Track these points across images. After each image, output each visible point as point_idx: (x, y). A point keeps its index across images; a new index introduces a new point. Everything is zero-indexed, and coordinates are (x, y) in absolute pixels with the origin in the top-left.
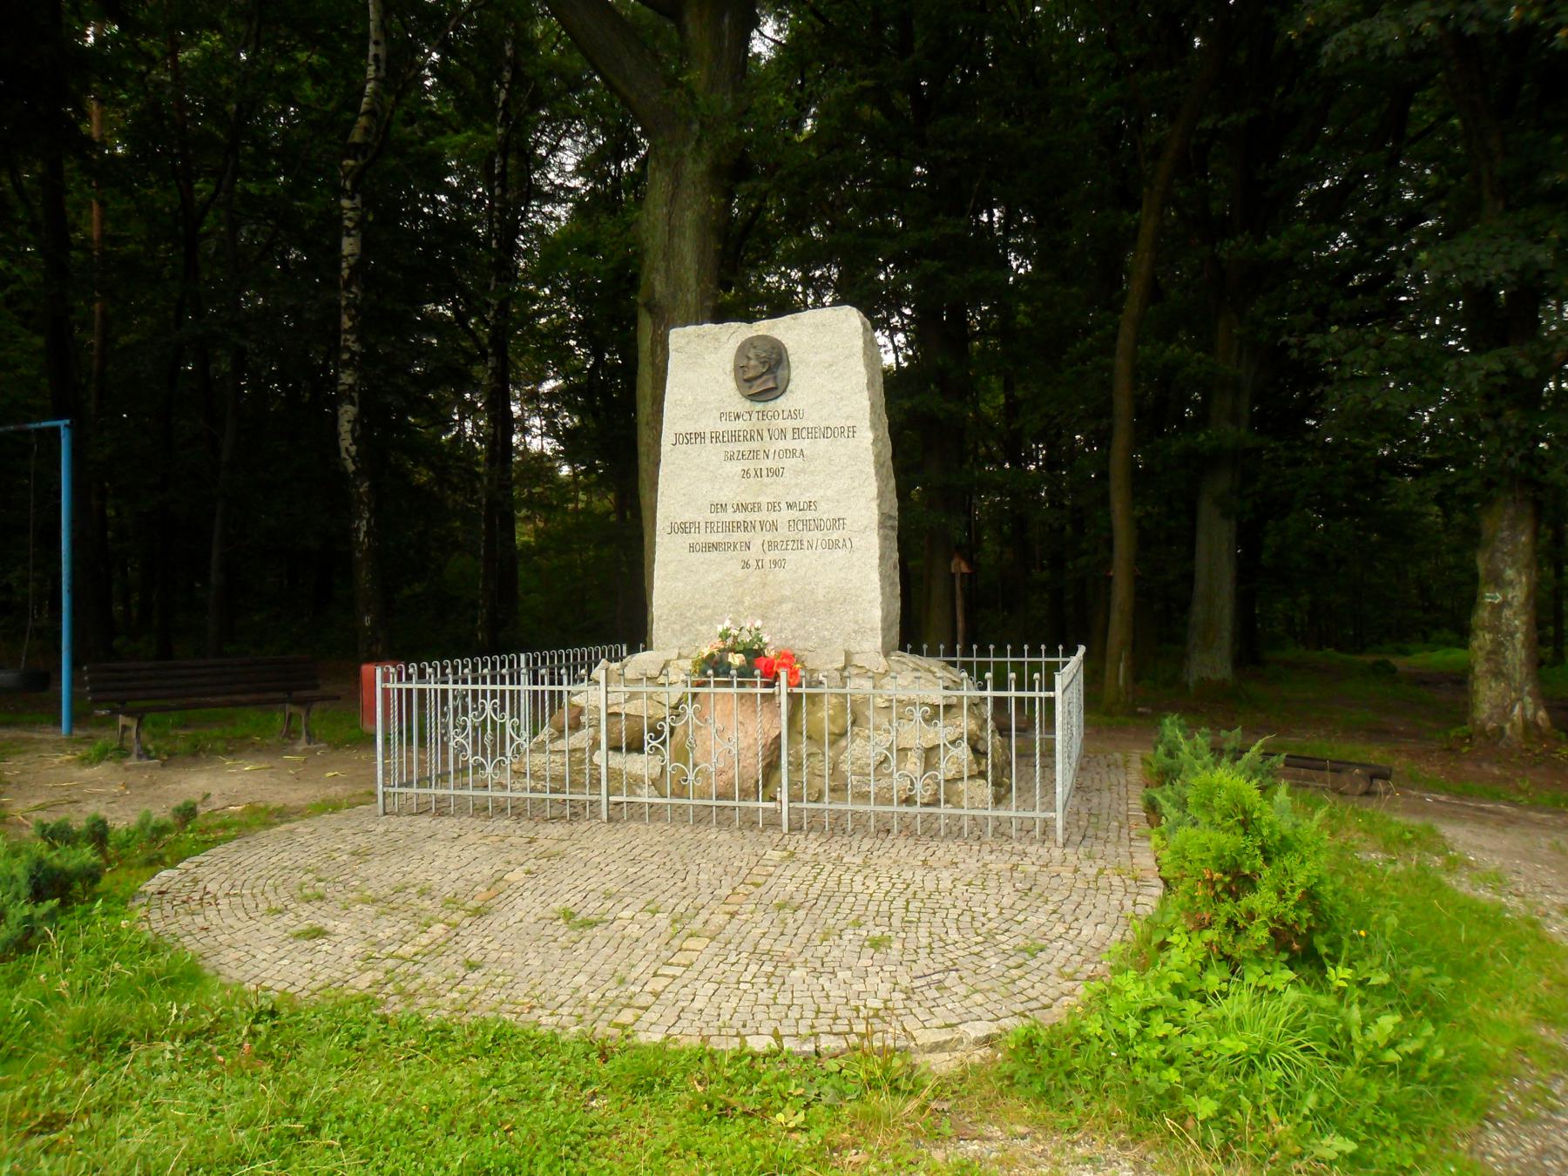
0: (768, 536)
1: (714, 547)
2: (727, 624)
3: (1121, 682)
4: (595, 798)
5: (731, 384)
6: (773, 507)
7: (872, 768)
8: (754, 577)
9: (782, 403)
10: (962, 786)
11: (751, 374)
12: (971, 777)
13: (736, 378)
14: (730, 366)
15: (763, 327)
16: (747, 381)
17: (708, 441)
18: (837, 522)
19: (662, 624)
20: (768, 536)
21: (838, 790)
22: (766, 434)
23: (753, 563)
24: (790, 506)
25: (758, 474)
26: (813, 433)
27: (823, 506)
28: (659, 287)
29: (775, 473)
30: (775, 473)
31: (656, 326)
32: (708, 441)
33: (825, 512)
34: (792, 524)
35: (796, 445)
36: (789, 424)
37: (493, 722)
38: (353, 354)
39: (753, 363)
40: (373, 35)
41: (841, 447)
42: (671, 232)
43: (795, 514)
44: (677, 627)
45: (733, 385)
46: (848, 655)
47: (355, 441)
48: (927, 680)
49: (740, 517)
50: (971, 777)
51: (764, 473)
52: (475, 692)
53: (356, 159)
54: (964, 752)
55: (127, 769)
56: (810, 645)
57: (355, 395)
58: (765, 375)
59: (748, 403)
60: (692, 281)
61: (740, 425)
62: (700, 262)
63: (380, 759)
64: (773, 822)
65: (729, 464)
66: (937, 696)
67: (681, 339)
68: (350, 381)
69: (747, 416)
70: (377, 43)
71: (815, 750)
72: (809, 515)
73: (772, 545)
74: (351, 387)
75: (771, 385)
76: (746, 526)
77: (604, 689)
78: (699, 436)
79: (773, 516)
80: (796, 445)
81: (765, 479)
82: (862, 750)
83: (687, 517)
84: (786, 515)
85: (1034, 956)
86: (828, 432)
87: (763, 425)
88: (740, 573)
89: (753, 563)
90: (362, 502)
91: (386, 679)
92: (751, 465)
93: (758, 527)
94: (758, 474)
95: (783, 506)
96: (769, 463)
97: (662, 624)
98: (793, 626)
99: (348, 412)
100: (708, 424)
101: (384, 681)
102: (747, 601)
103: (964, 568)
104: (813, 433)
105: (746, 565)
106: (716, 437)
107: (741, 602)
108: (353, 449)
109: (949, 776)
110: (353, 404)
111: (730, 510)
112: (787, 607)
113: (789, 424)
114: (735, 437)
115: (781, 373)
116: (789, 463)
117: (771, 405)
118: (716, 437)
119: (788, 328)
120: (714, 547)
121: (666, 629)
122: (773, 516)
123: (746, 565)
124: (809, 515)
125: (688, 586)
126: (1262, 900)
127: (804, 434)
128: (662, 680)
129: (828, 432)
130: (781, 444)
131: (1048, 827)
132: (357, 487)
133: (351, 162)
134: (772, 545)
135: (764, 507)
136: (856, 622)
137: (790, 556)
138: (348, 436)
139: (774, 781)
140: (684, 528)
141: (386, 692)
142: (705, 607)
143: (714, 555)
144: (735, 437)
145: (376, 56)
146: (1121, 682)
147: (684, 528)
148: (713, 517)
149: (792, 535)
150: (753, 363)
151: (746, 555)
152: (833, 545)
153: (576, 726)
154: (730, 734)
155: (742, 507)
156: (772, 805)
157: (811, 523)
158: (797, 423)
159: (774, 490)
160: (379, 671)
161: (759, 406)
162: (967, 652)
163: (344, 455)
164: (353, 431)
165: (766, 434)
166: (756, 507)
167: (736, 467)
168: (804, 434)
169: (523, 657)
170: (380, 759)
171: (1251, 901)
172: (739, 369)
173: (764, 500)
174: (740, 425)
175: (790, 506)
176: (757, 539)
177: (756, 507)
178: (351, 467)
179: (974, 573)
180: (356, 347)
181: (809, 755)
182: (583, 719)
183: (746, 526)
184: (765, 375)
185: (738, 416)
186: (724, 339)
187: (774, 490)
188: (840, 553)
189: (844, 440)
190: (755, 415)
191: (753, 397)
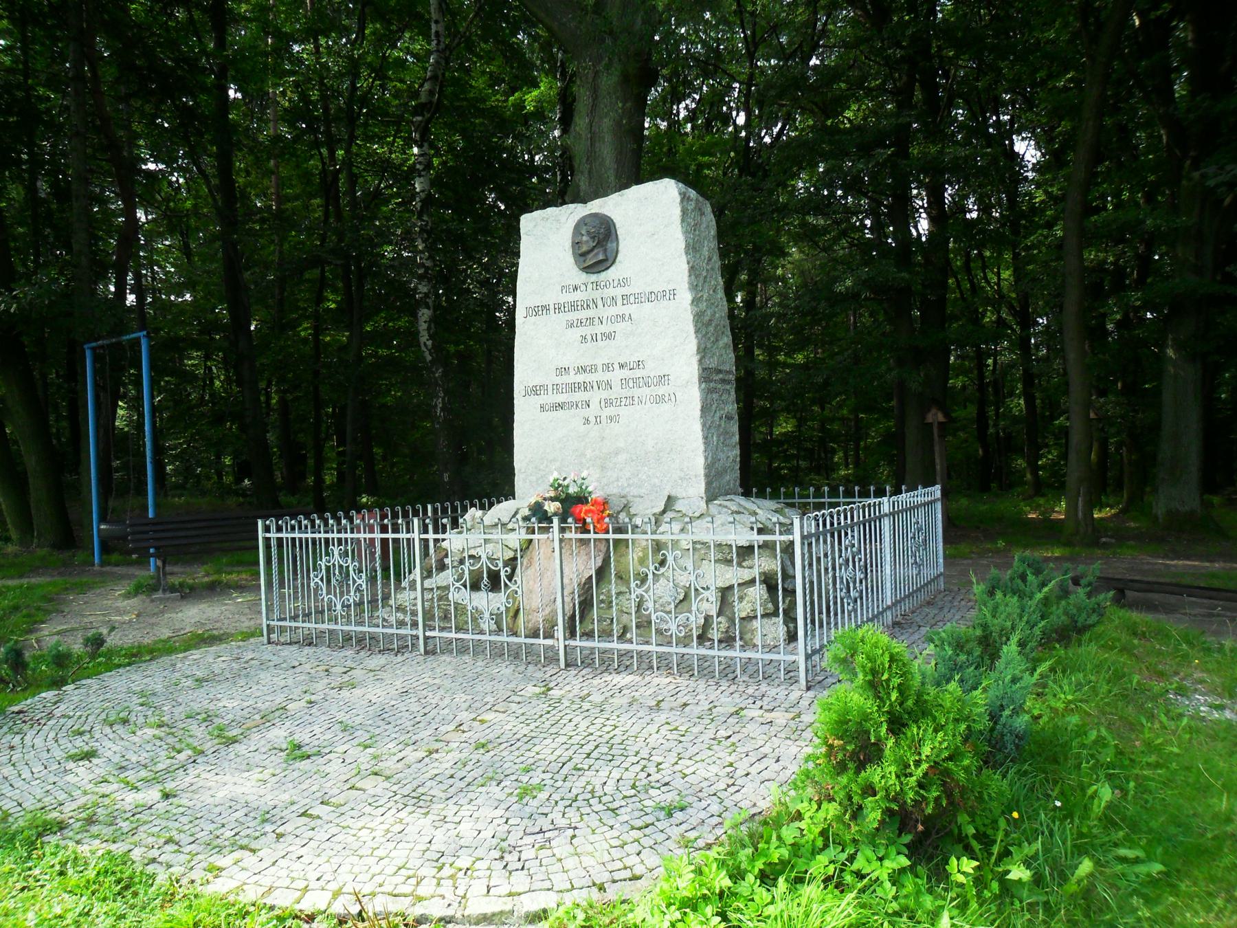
1: (560, 406)
2: (556, 475)
3: (1080, 514)
4: (414, 632)
5: (569, 259)
6: (608, 367)
7: (672, 606)
8: (594, 430)
9: (612, 273)
10: (756, 624)
11: (585, 248)
12: (763, 616)
14: (568, 244)
15: (595, 206)
16: (583, 255)
17: (552, 311)
18: (663, 379)
19: (522, 476)
20: (604, 394)
21: (644, 624)
22: (600, 303)
23: (592, 419)
24: (622, 366)
25: (594, 338)
26: (638, 298)
27: (649, 365)
29: (609, 336)
30: (609, 336)
32: (552, 311)
33: (652, 369)
34: (624, 382)
35: (626, 310)
36: (619, 292)
37: (341, 566)
38: (427, 268)
39: (585, 238)
40: (434, 16)
41: (662, 309)
42: (592, 140)
43: (626, 373)
45: (572, 260)
46: (670, 500)
47: (431, 337)
48: (738, 522)
49: (580, 378)
50: (763, 616)
51: (599, 337)
52: (327, 540)
53: (423, 115)
54: (758, 593)
55: (152, 601)
56: (643, 491)
57: (430, 301)
58: (597, 247)
59: (584, 277)
60: (612, 178)
62: (618, 162)
63: (263, 597)
64: (552, 659)
66: (746, 537)
67: (529, 223)
68: (425, 290)
69: (583, 287)
70: (437, 22)
71: (624, 589)
72: (638, 373)
73: (609, 402)
74: (427, 295)
75: (601, 257)
76: (585, 387)
77: (480, 534)
78: (545, 308)
79: (607, 376)
80: (626, 310)
82: (661, 592)
83: (537, 381)
84: (619, 374)
85: (670, 815)
86: (652, 297)
87: (597, 295)
88: (583, 428)
89: (592, 419)
90: (437, 384)
91: (267, 529)
92: (587, 331)
93: (596, 387)
94: (594, 338)
95: (616, 366)
96: (600, 329)
97: (522, 476)
98: (628, 475)
99: (425, 314)
100: (553, 297)
101: (266, 532)
102: (589, 453)
103: (941, 417)
104: (638, 298)
105: (587, 421)
106: (559, 308)
107: (584, 455)
108: (429, 343)
109: (743, 615)
110: (428, 308)
111: (572, 372)
112: (622, 457)
113: (619, 292)
114: (574, 306)
115: (611, 246)
116: (619, 327)
117: (603, 274)
118: (559, 308)
120: (560, 406)
121: (525, 481)
122: (607, 376)
123: (587, 421)
124: (638, 373)
125: (543, 444)
126: (882, 775)
127: (632, 298)
128: (510, 526)
129: (652, 297)
130: (613, 311)
131: (791, 670)
132: (434, 373)
133: (419, 118)
134: (609, 402)
135: (600, 368)
136: (682, 470)
137: (623, 411)
138: (425, 333)
139: (588, 620)
140: (535, 391)
141: (267, 540)
142: (554, 460)
144: (574, 306)
145: (437, 32)
146: (1080, 514)
147: (535, 391)
148: (559, 380)
149: (625, 393)
150: (585, 238)
152: (659, 400)
153: (442, 567)
154: (552, 574)
155: (583, 369)
156: (549, 642)
157: (641, 380)
158: (625, 291)
159: (605, 353)
160: (260, 522)
161: (594, 277)
163: (424, 349)
164: (429, 329)
165: (600, 303)
166: (593, 369)
167: (577, 333)
168: (632, 298)
169: (429, 507)
170: (263, 597)
171: (874, 774)
172: (576, 244)
173: (599, 362)
174: (578, 296)
175: (622, 366)
176: (595, 396)
177: (593, 369)
178: (429, 358)
179: (793, 423)
180: (428, 263)
181: (618, 594)
182: (447, 561)
183: (585, 387)
185: (576, 288)
186: (563, 219)
187: (605, 353)
188: (665, 407)
189: (666, 302)
190: (590, 286)
191: (588, 269)
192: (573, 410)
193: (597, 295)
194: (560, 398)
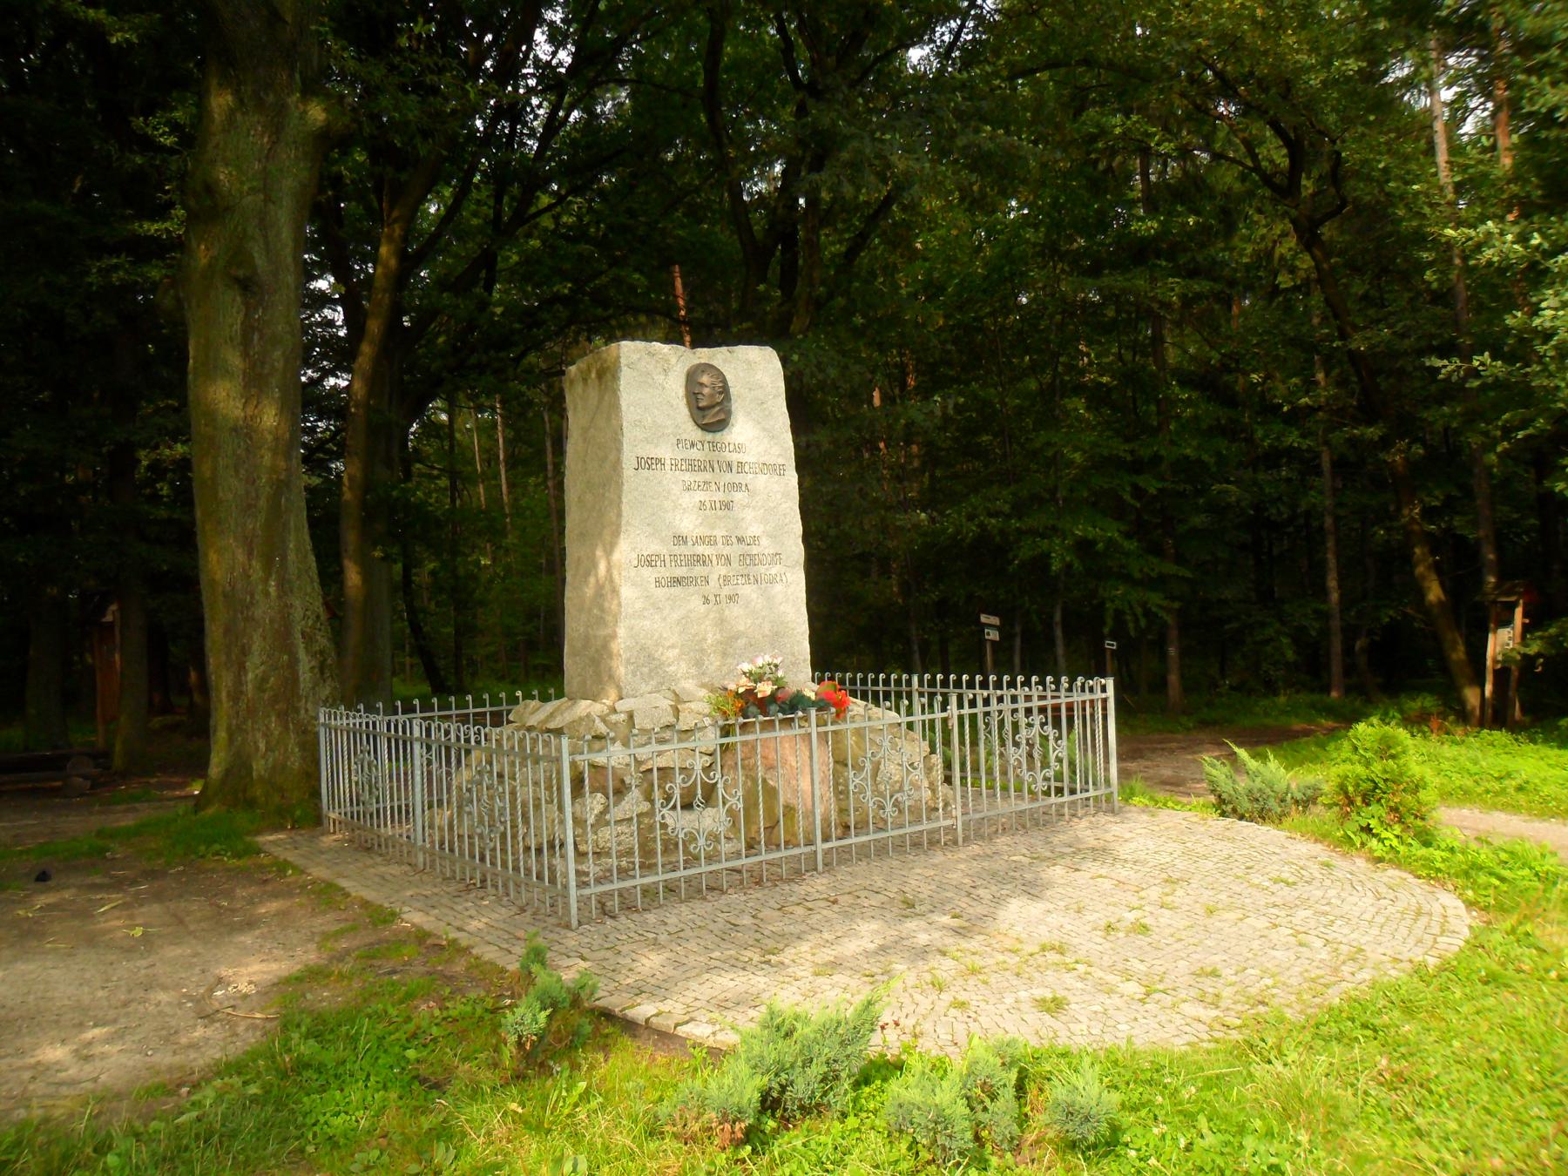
0: (723, 571)
1: (678, 581)
13: (689, 404)
15: (704, 355)
17: (668, 467)
23: (712, 598)
28: (260, 261)
31: (249, 310)
44: (646, 670)
61: (694, 454)
65: (687, 494)
81: (720, 513)
87: (714, 456)
119: (725, 361)
120: (678, 581)
122: (726, 550)
123: (706, 600)
143: (676, 591)
148: (678, 550)
151: (706, 589)
161: (709, 437)
162: (445, 706)
174: (694, 454)
184: (710, 409)
185: (693, 445)
191: (706, 428)
192: (692, 589)
193: (714, 456)
194: (681, 572)
